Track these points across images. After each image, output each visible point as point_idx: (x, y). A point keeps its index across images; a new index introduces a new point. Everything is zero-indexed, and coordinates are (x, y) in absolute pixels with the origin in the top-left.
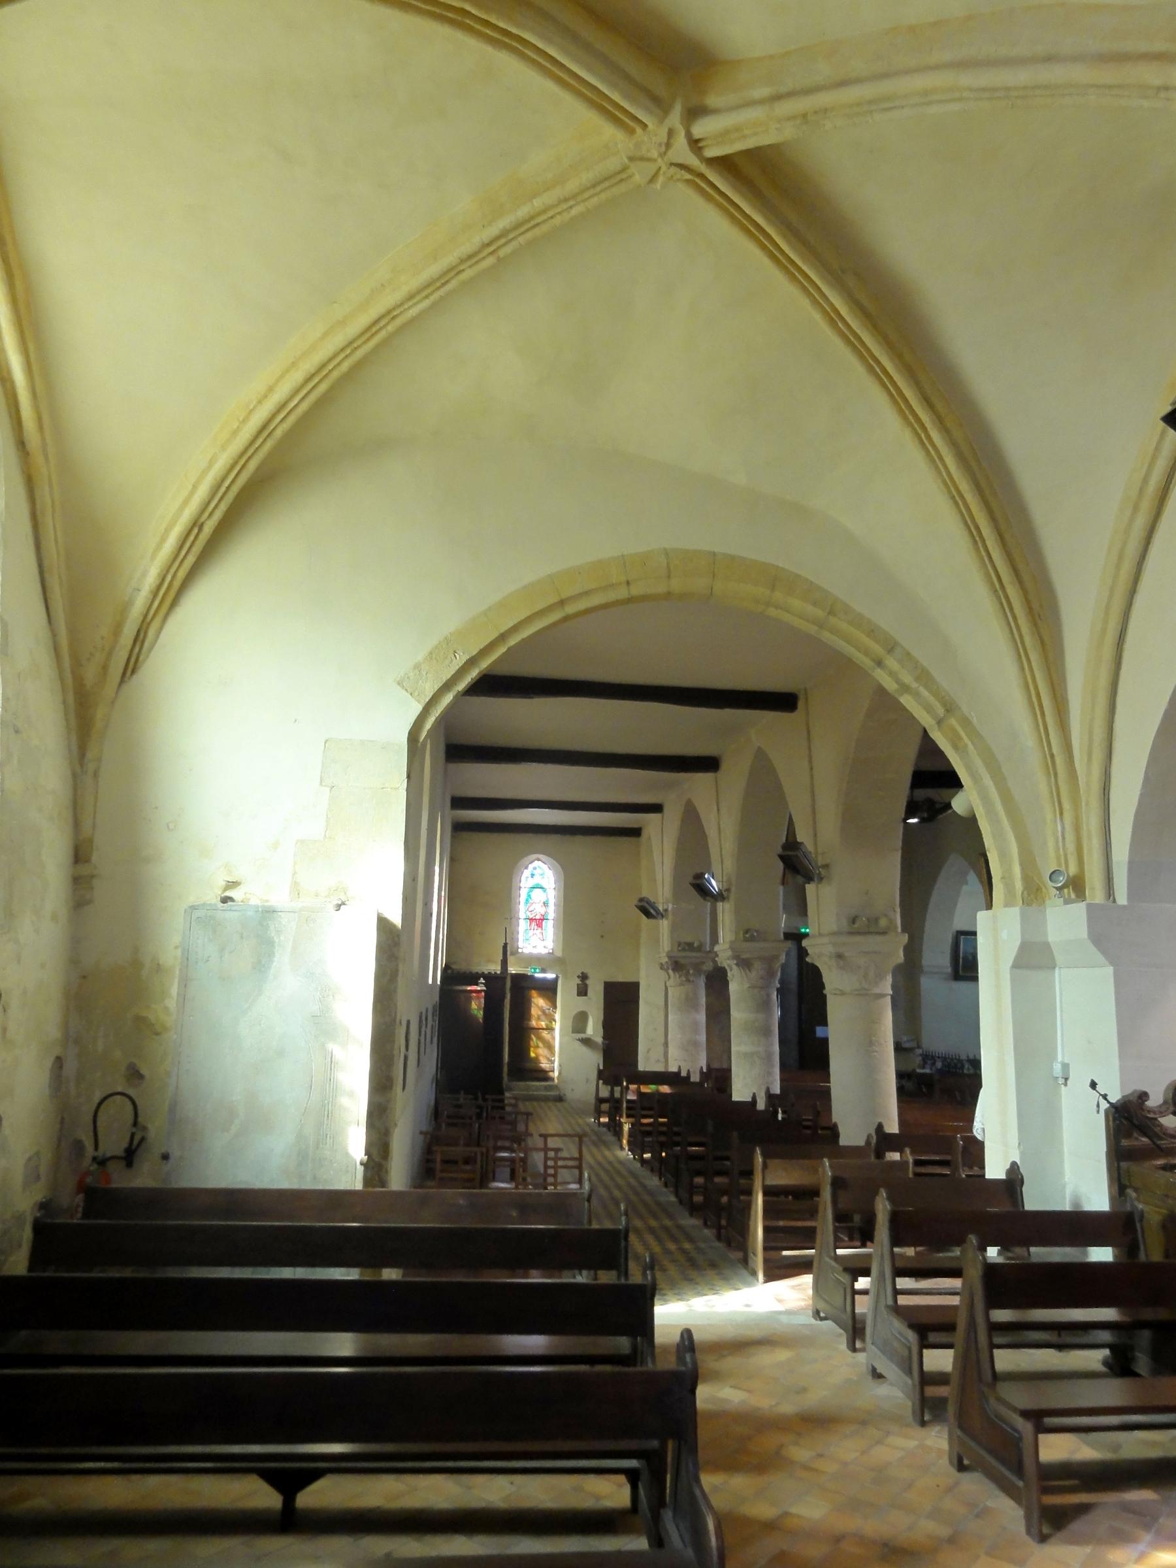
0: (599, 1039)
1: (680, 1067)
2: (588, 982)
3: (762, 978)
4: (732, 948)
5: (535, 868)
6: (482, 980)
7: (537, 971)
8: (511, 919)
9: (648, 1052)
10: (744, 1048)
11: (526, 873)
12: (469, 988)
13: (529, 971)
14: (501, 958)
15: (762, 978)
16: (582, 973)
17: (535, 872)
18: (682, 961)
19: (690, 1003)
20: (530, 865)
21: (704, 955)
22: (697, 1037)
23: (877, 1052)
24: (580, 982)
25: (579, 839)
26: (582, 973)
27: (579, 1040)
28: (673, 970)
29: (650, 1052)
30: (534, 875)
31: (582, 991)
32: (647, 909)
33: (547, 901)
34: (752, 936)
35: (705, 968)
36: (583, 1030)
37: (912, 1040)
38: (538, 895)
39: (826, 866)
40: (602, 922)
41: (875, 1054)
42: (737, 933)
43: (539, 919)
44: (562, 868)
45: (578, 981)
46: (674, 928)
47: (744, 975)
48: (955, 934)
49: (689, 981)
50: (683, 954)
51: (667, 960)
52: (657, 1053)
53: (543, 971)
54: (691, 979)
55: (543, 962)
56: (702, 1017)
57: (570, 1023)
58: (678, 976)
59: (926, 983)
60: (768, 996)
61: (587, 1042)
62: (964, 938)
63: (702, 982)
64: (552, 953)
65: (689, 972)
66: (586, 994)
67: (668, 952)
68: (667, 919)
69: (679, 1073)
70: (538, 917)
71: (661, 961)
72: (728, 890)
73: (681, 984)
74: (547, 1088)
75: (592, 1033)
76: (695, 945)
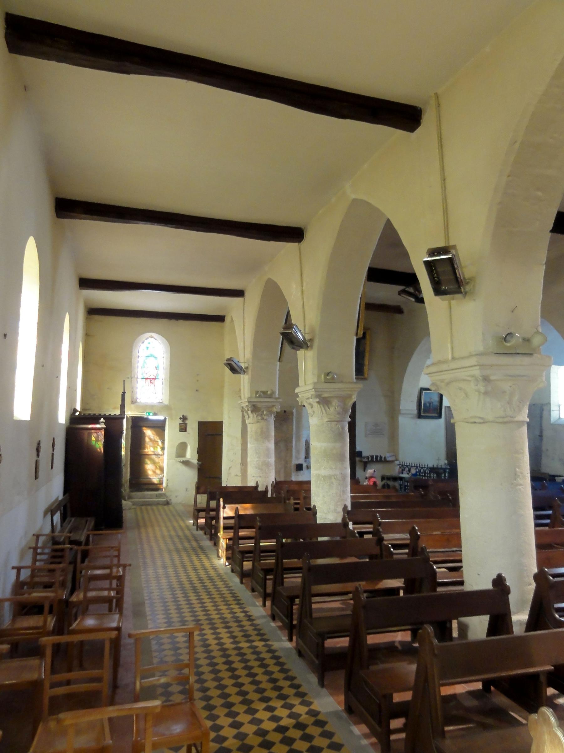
0: (195, 461)
1: (257, 483)
2: (187, 422)
4: (315, 389)
6: (102, 420)
7: (151, 414)
8: (132, 378)
9: (229, 469)
10: (324, 472)
12: (90, 426)
13: (145, 415)
15: (338, 413)
16: (183, 416)
17: (148, 346)
18: (259, 405)
19: (263, 435)
21: (275, 400)
22: (269, 460)
23: (521, 485)
25: (181, 322)
26: (183, 416)
27: (181, 462)
28: (252, 411)
29: (231, 469)
31: (183, 428)
32: (234, 369)
33: (158, 366)
34: (333, 378)
36: (184, 455)
37: (394, 455)
38: (151, 363)
39: (472, 279)
41: (520, 487)
42: (319, 377)
43: (152, 379)
46: (253, 381)
47: (324, 412)
48: (420, 389)
50: (259, 400)
51: (247, 404)
52: (237, 470)
53: (155, 414)
54: (265, 418)
55: (155, 409)
56: (272, 445)
58: (255, 416)
60: (343, 428)
61: (186, 463)
62: (425, 393)
63: (272, 420)
64: (162, 402)
65: (263, 412)
66: (185, 431)
68: (248, 374)
69: (256, 487)
71: (242, 405)
72: (311, 340)
73: (258, 422)
75: (190, 457)
76: (269, 393)
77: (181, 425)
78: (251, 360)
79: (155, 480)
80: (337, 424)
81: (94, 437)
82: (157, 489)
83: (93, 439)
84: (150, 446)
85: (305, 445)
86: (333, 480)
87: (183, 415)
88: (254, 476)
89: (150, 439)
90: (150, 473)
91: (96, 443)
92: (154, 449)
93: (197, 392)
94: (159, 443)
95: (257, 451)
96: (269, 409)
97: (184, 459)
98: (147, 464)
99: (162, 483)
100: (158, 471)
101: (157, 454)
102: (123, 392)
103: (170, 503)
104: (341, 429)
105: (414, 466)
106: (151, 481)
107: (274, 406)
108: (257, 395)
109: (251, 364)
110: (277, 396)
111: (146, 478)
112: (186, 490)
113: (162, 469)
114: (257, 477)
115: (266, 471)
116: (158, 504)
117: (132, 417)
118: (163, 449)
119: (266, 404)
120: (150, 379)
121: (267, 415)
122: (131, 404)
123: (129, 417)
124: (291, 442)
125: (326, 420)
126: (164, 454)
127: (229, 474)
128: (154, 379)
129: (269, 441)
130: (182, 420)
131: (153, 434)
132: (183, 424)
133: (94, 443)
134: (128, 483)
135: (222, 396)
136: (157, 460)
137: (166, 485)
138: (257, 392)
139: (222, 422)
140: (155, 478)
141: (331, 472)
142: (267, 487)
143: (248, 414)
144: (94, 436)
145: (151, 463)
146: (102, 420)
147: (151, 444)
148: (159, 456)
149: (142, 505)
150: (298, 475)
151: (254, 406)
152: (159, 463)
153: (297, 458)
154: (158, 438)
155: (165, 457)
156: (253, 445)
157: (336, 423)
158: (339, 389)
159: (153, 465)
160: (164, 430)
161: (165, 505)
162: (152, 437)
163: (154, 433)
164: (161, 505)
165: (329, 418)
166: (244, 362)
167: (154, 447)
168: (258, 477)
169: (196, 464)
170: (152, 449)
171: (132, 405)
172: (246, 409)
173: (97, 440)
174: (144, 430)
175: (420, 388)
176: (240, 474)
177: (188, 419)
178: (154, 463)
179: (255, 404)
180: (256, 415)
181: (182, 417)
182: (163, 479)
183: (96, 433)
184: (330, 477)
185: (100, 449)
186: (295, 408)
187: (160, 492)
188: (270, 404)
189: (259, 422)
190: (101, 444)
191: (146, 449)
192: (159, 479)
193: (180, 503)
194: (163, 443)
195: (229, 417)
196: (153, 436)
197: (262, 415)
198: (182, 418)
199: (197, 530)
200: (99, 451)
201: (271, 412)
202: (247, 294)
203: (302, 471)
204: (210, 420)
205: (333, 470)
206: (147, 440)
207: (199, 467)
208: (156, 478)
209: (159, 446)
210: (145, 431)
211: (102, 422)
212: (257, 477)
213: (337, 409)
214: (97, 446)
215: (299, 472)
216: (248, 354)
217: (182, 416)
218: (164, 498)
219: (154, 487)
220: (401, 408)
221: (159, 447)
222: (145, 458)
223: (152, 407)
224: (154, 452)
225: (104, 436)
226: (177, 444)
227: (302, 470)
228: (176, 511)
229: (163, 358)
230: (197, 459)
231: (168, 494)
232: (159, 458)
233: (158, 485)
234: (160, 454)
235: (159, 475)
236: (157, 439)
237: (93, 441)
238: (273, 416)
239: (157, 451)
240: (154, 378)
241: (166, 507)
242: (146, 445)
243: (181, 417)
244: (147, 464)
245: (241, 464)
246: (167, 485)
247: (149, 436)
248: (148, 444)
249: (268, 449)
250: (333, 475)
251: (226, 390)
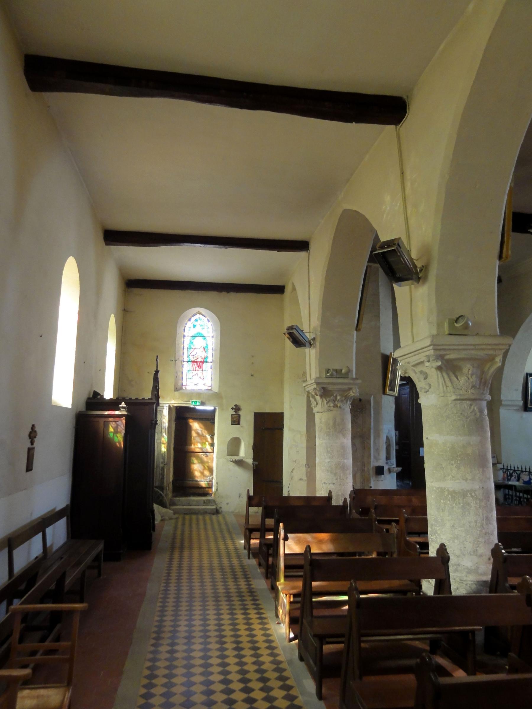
0: (250, 461)
1: (330, 492)
2: (240, 413)
3: (474, 387)
4: (435, 346)
5: (196, 320)
6: (123, 404)
7: (198, 404)
8: (176, 361)
9: (292, 472)
10: (450, 485)
11: (189, 324)
12: (107, 413)
13: (191, 405)
14: (152, 386)
15: (474, 387)
16: (236, 406)
17: (196, 323)
18: (330, 387)
20: (192, 318)
21: (352, 382)
22: (345, 461)
24: (234, 413)
25: (233, 295)
26: (236, 406)
27: (233, 461)
28: (321, 396)
29: (294, 471)
30: (196, 326)
31: (236, 421)
33: (207, 346)
34: (466, 327)
35: (352, 394)
36: (237, 454)
38: (199, 342)
40: (252, 363)
42: (439, 325)
43: (200, 362)
44: (219, 318)
45: (232, 412)
46: (322, 357)
47: (449, 383)
49: (337, 406)
51: (315, 386)
52: (301, 472)
53: (203, 404)
54: (339, 405)
55: (204, 400)
56: (348, 441)
57: (225, 448)
58: (325, 402)
59: (504, 413)
60: (481, 411)
61: (240, 463)
63: (347, 408)
64: (211, 390)
65: (336, 397)
66: (239, 424)
67: (317, 378)
68: (314, 347)
69: (329, 499)
70: (198, 360)
71: (307, 390)
74: (206, 503)
75: (244, 456)
76: (343, 371)
77: (233, 416)
78: (319, 329)
79: (203, 483)
80: (471, 405)
81: (112, 427)
82: (206, 494)
83: (111, 429)
84: (197, 442)
85: (386, 442)
86: (469, 499)
87: (236, 404)
88: (325, 483)
89: (198, 433)
90: (197, 474)
91: (115, 435)
92: (202, 445)
93: (253, 377)
94: (207, 438)
95: (329, 449)
96: (344, 393)
97: (236, 458)
98: (194, 463)
99: (210, 486)
100: (207, 473)
101: (205, 451)
102: (155, 371)
103: (220, 511)
104: (478, 414)
105: (526, 472)
106: (199, 484)
107: (350, 389)
108: (328, 375)
109: (319, 334)
110: (354, 376)
111: (193, 481)
112: (240, 496)
113: (211, 470)
114: (329, 484)
115: (342, 476)
116: (205, 512)
117: (176, 407)
118: (212, 445)
120: (198, 362)
121: (342, 401)
122: (175, 391)
123: (172, 406)
124: (369, 438)
125: (454, 397)
126: (213, 452)
127: (292, 478)
128: (203, 362)
129: (344, 436)
130: (234, 410)
131: (201, 427)
132: (235, 416)
133: (111, 435)
134: (171, 486)
135: (282, 382)
136: (205, 459)
137: (215, 490)
138: (328, 371)
139: (283, 413)
140: (203, 480)
141: (466, 486)
142: (345, 500)
143: (315, 400)
144: (112, 425)
145: (199, 463)
146: (123, 404)
147: (198, 439)
148: (207, 454)
149: (187, 514)
150: (378, 481)
151: (323, 388)
152: (208, 462)
153: (377, 459)
154: (206, 432)
155: (215, 455)
156: (324, 441)
157: (469, 402)
159: (200, 464)
160: (214, 423)
161: (213, 514)
162: (200, 432)
163: (202, 426)
164: (210, 513)
165: (457, 395)
166: (310, 333)
167: (203, 443)
168: (331, 484)
169: (252, 464)
170: (199, 445)
171: (176, 393)
172: (313, 393)
173: (116, 432)
174: (190, 422)
175: (526, 374)
177: (241, 409)
178: (202, 462)
179: (324, 386)
180: (326, 401)
181: (234, 407)
182: (212, 482)
183: (114, 421)
184: (464, 494)
185: (120, 443)
186: (372, 396)
187: (208, 498)
188: (345, 387)
189: (331, 410)
190: (121, 437)
191: (192, 445)
192: (207, 481)
193: (232, 512)
194: (212, 438)
195: (291, 407)
196: (202, 429)
198: (234, 409)
199: (249, 558)
200: (118, 446)
201: (346, 398)
202: (312, 246)
203: (383, 476)
204: (268, 411)
205: (468, 481)
206: (194, 434)
207: (255, 468)
208: (204, 480)
209: (208, 442)
210: (191, 424)
211: (123, 408)
212: (329, 484)
213: (471, 379)
214: (116, 439)
215: (379, 476)
216: (316, 321)
217: (235, 406)
218: (214, 506)
219: (200, 491)
220: (502, 398)
221: (207, 443)
222: (191, 457)
223: (199, 394)
224: (201, 448)
225: (125, 425)
226: (229, 439)
227: (383, 474)
228: (226, 523)
229: (213, 337)
231: (218, 500)
232: (208, 456)
233: (207, 489)
234: (209, 452)
235: (207, 477)
236: (206, 433)
237: (111, 432)
238: (349, 403)
239: (206, 448)
240: (202, 361)
241: (214, 517)
242: (192, 440)
243: (233, 407)
244: (194, 463)
245: (307, 466)
246: (217, 490)
247: (197, 430)
248: (194, 439)
249: (343, 447)
250: (468, 491)
251: (287, 375)
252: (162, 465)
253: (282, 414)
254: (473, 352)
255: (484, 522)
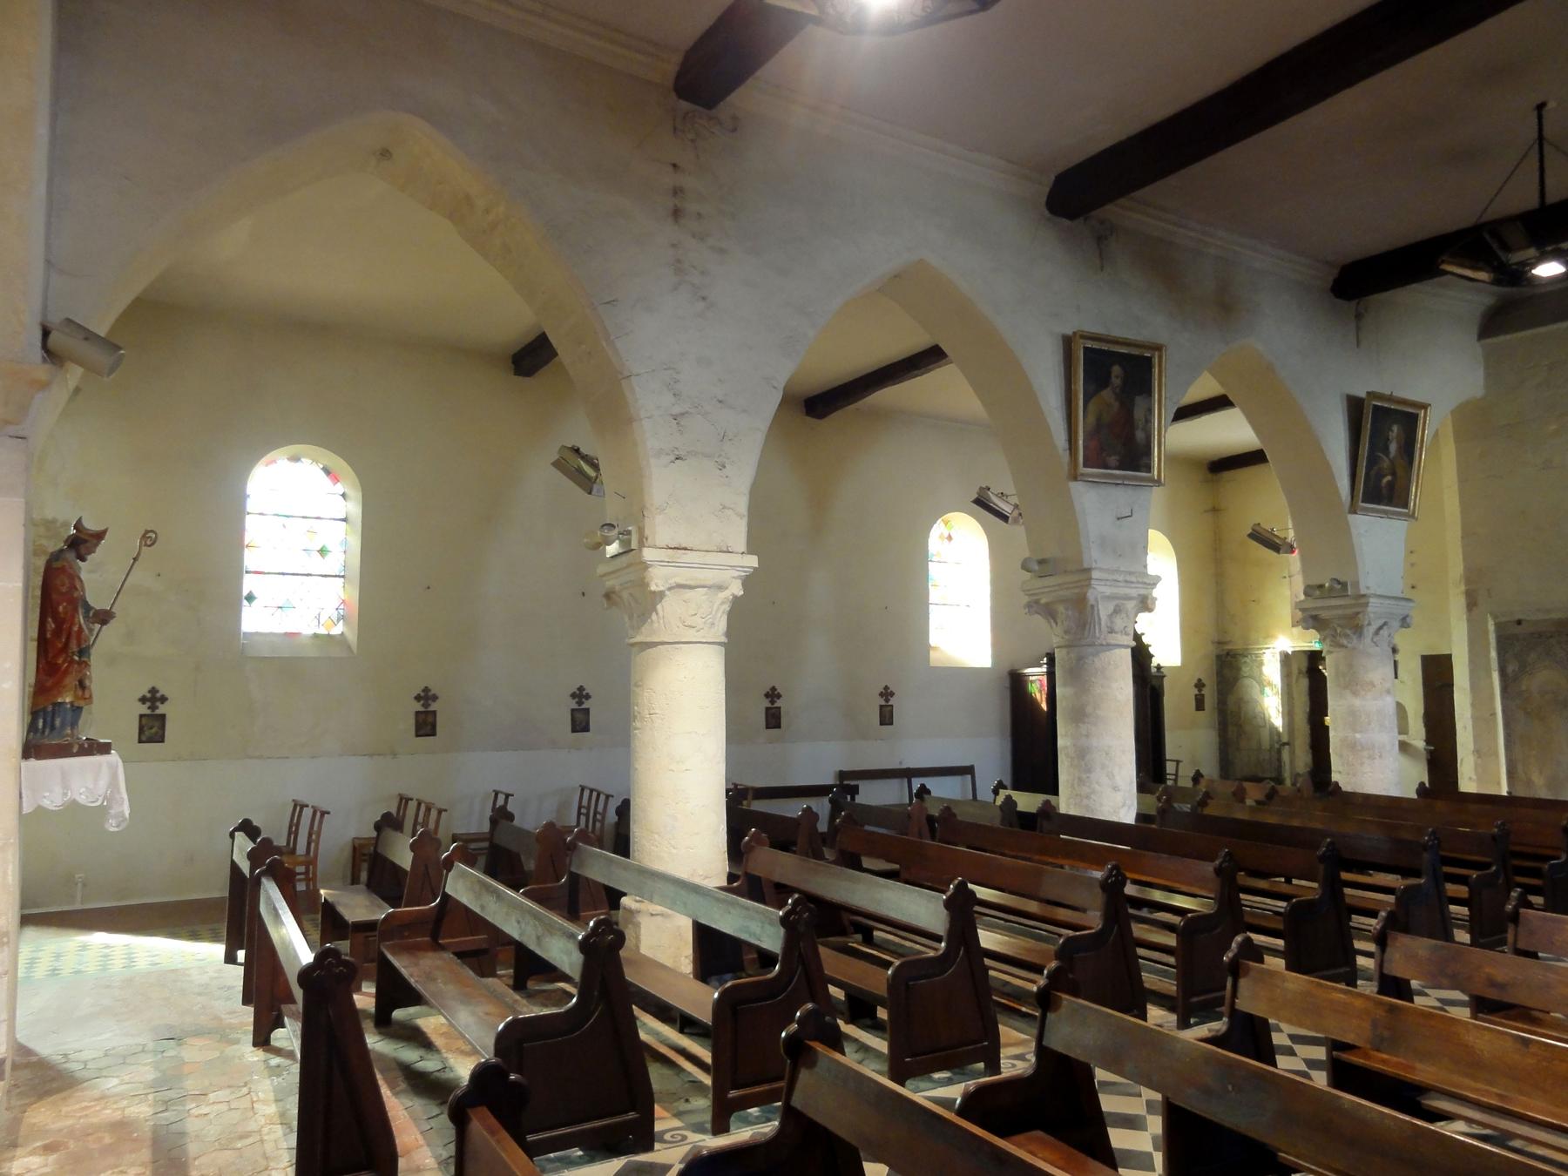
18: (1324, 614)
21: (1353, 602)
50: (1320, 603)
65: (1336, 631)
76: (1327, 585)
115: (1350, 759)
119: (1340, 612)
121: (1347, 636)
122: (1293, 626)
151: (1315, 618)
158: (1059, 585)
176: (1474, 777)
179: (1314, 613)
188: (1349, 611)
197: (1333, 636)
230: (1424, 738)
252: (1277, 746)
253: (1449, 657)
254: (1061, 593)
255: (1076, 781)
